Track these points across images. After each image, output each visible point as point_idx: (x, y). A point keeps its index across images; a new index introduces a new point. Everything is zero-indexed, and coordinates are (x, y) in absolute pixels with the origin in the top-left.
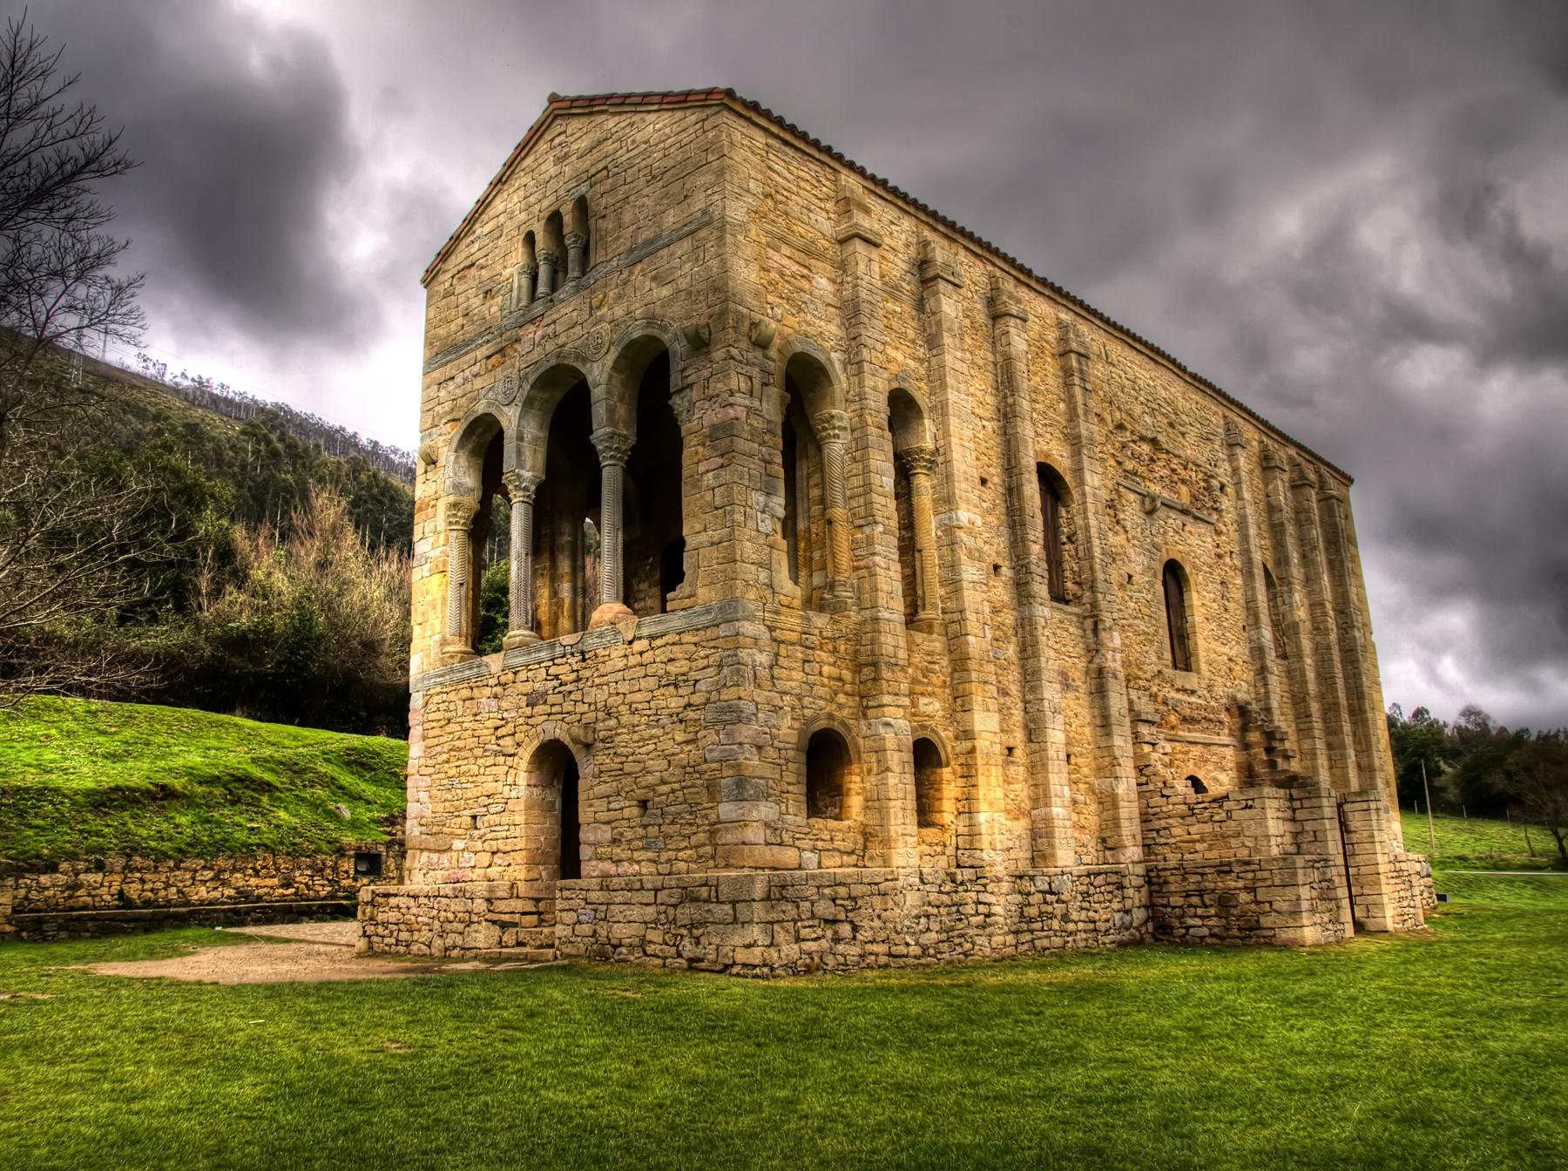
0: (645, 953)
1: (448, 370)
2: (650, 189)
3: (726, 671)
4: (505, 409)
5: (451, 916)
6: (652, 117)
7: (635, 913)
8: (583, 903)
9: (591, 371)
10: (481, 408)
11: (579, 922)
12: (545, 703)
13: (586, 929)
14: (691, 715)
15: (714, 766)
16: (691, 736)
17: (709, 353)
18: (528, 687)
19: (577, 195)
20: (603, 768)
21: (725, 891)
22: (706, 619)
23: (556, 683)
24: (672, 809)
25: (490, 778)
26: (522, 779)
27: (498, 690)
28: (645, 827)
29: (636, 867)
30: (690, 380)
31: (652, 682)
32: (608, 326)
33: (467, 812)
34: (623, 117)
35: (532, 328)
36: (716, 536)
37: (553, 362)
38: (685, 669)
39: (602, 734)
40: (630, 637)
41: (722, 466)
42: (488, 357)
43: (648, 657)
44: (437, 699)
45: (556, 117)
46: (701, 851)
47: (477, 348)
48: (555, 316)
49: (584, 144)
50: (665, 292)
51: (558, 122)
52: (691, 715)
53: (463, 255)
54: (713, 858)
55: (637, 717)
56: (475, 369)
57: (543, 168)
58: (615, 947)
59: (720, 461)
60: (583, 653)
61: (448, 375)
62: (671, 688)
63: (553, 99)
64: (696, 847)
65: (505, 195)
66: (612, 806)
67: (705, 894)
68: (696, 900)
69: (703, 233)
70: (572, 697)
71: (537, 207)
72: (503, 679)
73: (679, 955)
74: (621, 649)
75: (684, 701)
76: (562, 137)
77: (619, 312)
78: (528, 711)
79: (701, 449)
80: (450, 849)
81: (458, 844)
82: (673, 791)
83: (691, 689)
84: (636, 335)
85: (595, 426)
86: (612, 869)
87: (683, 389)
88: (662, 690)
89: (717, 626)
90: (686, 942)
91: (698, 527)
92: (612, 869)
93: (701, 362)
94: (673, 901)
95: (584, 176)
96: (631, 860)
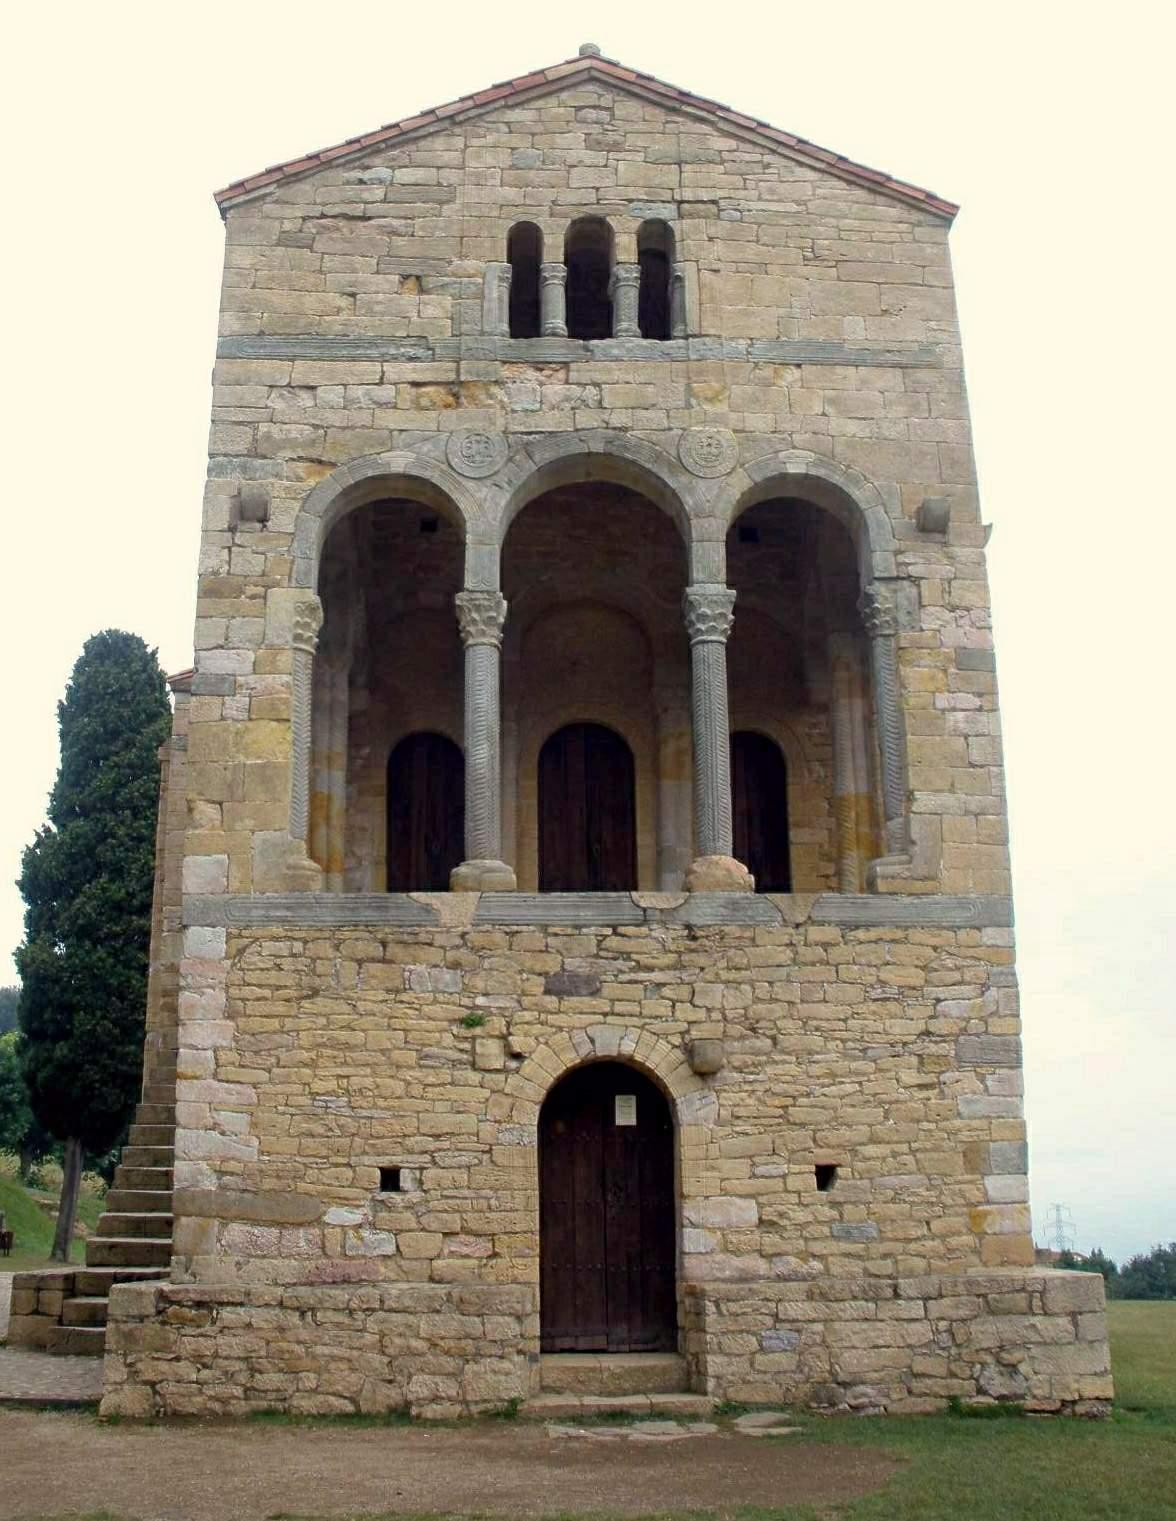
0: (910, 1392)
1: (301, 371)
2: (805, 271)
3: (993, 992)
4: (470, 484)
5: (418, 1344)
6: (811, 175)
7: (885, 1333)
8: (769, 1321)
9: (691, 491)
10: (399, 462)
11: (762, 1349)
12: (595, 993)
13: (785, 1361)
14: (933, 1048)
15: (975, 1123)
16: (930, 1078)
17: (945, 544)
18: (552, 964)
19: (649, 215)
20: (741, 1112)
21: (1058, 1300)
22: (958, 917)
23: (620, 964)
24: (894, 1181)
25: (440, 1106)
26: (531, 1117)
27: (463, 955)
28: (834, 1204)
29: (817, 1265)
30: (913, 570)
31: (853, 993)
32: (729, 434)
33: (366, 1160)
34: (749, 147)
35: (531, 374)
36: (974, 803)
37: (598, 447)
38: (913, 982)
39: (736, 1061)
40: (801, 919)
41: (980, 709)
42: (416, 384)
43: (835, 954)
44: (269, 947)
45: (593, 80)
46: (954, 1241)
47: (384, 359)
48: (598, 377)
49: (662, 146)
50: (852, 427)
51: (590, 87)
52: (933, 1048)
53: (336, 194)
54: (976, 1252)
55: (816, 1040)
56: (386, 393)
57: (559, 140)
58: (844, 1385)
59: (977, 702)
60: (688, 927)
61: (298, 378)
62: (892, 1006)
63: (588, 53)
64: (943, 1237)
65: (459, 142)
66: (759, 1171)
67: (1023, 1304)
68: (1009, 1312)
69: (923, 375)
70: (666, 991)
71: (550, 194)
72: (475, 938)
73: (981, 1391)
74: (786, 934)
75: (921, 1026)
76: (605, 116)
77: (758, 422)
78: (551, 1001)
79: (941, 675)
80: (318, 1221)
81: (336, 1215)
82: (895, 1155)
83: (930, 1011)
84: (792, 469)
85: (697, 574)
86: (762, 1266)
87: (898, 578)
88: (873, 1006)
89: (979, 929)
90: (992, 1370)
91: (939, 784)
92: (762, 1266)
93: (934, 551)
94: (963, 1313)
95: (667, 196)
96: (807, 1256)
